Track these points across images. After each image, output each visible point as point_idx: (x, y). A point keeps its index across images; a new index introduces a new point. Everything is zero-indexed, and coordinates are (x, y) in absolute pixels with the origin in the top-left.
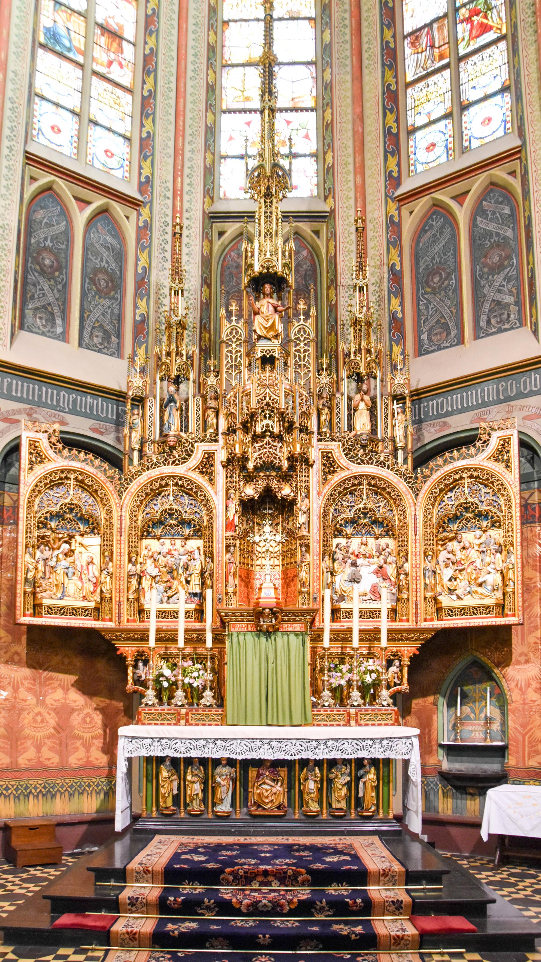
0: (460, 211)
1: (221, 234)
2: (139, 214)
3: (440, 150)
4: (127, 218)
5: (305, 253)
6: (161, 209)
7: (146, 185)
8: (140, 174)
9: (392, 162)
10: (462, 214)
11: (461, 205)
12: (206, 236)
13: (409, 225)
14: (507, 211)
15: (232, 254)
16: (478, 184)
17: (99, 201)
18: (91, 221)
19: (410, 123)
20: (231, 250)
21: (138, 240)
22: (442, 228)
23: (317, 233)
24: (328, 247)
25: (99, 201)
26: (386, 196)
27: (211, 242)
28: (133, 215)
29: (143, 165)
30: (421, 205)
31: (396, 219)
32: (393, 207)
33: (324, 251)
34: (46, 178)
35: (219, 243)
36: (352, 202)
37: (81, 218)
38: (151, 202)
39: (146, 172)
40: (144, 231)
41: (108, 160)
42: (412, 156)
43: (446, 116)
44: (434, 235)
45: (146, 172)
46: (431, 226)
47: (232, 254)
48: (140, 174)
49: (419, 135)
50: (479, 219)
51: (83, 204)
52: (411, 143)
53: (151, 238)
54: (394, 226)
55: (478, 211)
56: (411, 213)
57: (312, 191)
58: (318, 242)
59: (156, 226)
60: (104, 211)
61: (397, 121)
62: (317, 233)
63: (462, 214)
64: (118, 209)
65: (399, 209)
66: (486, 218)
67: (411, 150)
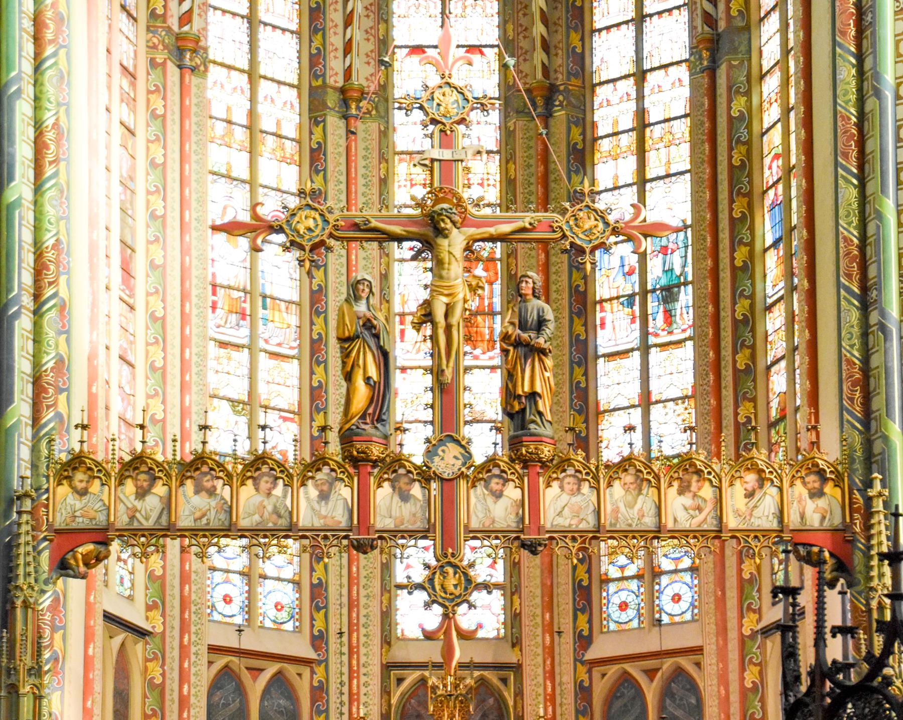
0: (649, 692)
1: (400, 681)
2: (313, 672)
3: (631, 613)
4: (299, 675)
5: (491, 701)
6: (337, 664)
7: (319, 640)
8: (312, 626)
9: (583, 619)
10: (651, 691)
11: (652, 680)
12: (386, 692)
13: (600, 689)
14: (693, 701)
15: (413, 701)
16: (668, 664)
17: (272, 669)
18: (266, 692)
19: (603, 570)
20: (410, 697)
21: (313, 701)
22: (634, 698)
23: (504, 681)
24: (515, 702)
25: (272, 669)
26: (575, 660)
27: (389, 694)
28: (306, 672)
29: (316, 615)
30: (613, 670)
31: (586, 684)
32: (582, 670)
33: (511, 703)
34: (221, 661)
35: (398, 693)
36: (540, 659)
37: (256, 688)
38: (326, 661)
39: (319, 625)
40: (319, 692)
41: (279, 615)
42: (604, 609)
43: (639, 577)
44: (625, 705)
45: (319, 625)
46: (623, 695)
47: (413, 701)
48: (312, 626)
49: (612, 587)
50: (668, 701)
51: (256, 673)
52: (604, 594)
53: (327, 701)
54: (584, 692)
55: (666, 693)
56: (604, 675)
57: (498, 630)
58: (506, 694)
59: (333, 688)
60: (279, 679)
61: (589, 571)
62: (504, 681)
63: (651, 691)
64: (291, 670)
65: (590, 671)
66: (674, 702)
67: (604, 601)
